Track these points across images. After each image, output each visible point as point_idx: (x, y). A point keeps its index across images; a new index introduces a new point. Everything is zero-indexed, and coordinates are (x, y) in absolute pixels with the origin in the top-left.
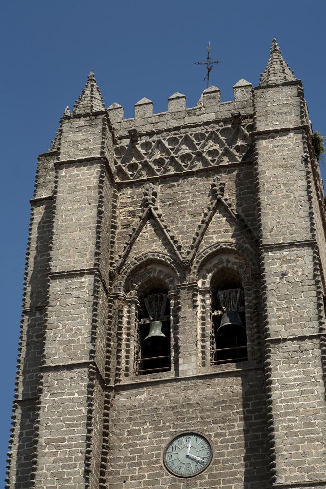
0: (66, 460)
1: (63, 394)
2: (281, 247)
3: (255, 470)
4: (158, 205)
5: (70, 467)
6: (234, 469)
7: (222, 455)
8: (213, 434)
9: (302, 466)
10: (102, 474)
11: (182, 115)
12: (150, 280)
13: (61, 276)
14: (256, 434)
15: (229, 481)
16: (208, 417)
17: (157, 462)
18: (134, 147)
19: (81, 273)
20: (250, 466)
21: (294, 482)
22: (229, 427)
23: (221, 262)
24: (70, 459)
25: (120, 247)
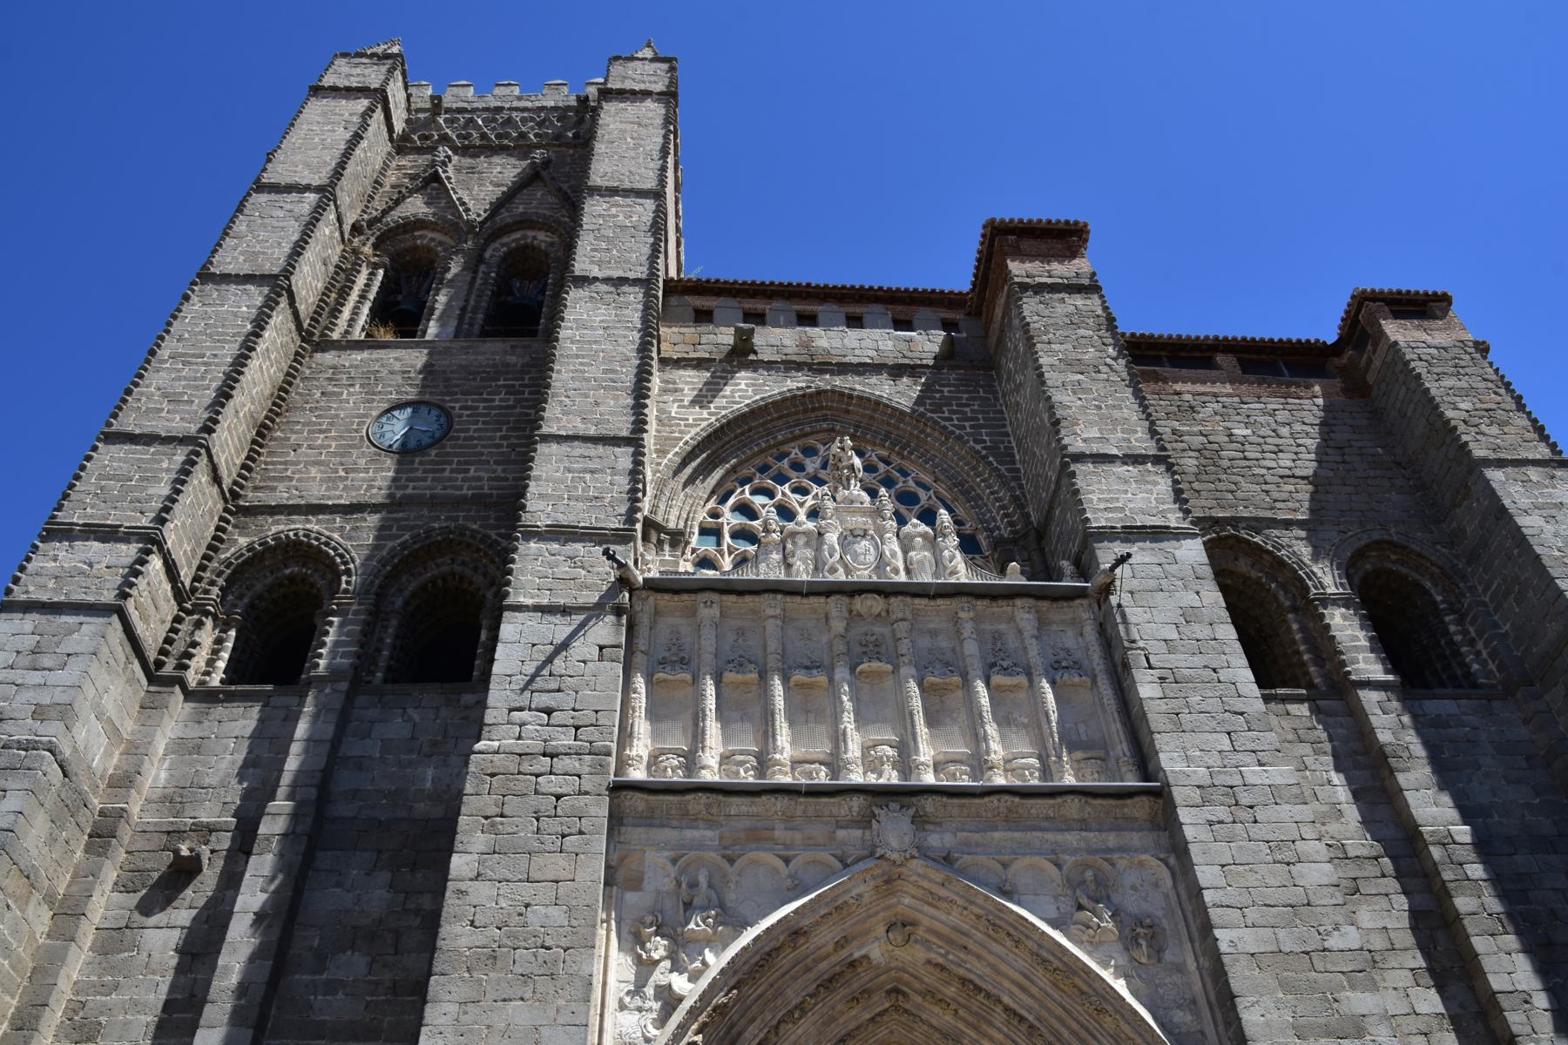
0: (195, 379)
1: (223, 305)
2: (613, 191)
4: (450, 168)
5: (197, 388)
6: (479, 449)
7: (467, 430)
8: (458, 405)
10: (259, 434)
11: (510, 99)
12: (416, 248)
13: (275, 188)
15: (467, 463)
16: (457, 386)
17: (356, 431)
18: (435, 121)
19: (307, 188)
22: (485, 400)
23: (525, 237)
24: (203, 378)
25: (379, 204)
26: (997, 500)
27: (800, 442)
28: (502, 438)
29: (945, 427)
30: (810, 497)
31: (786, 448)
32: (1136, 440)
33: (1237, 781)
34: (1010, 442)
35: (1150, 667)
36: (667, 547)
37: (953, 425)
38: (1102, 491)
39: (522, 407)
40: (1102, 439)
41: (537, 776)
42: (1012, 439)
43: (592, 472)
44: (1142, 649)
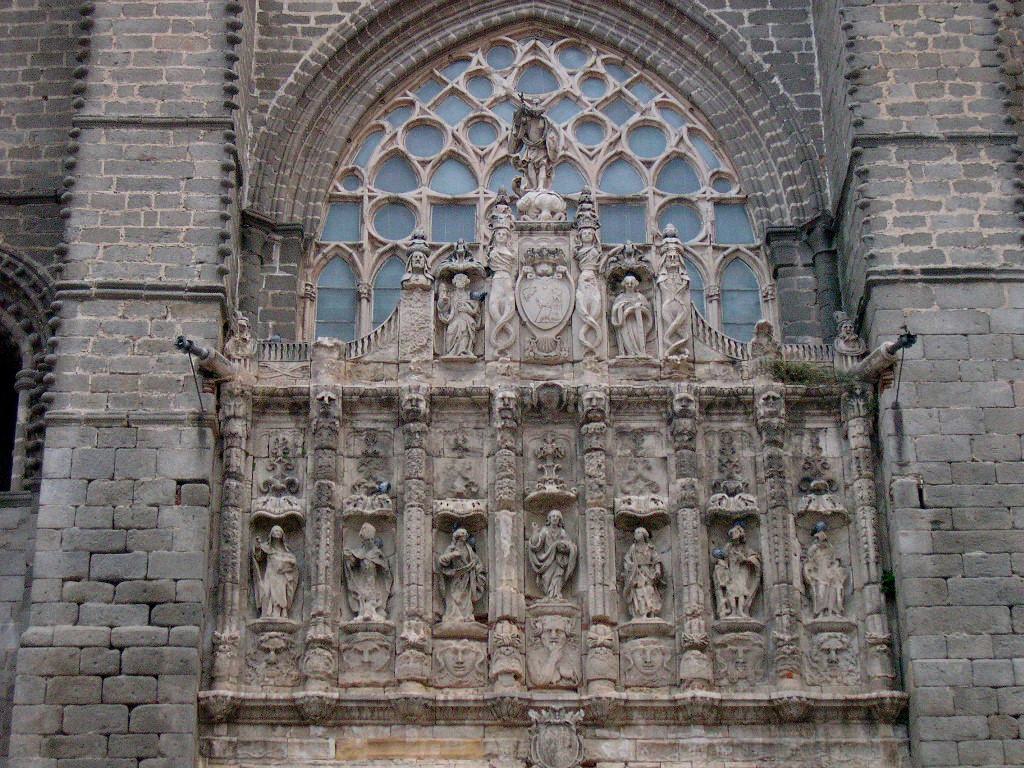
3: (45, 103)
9: (152, 83)
14: (62, 23)
20: (35, 93)
21: (125, 115)
26: (779, 152)
27: (484, 42)
28: (30, 75)
29: (710, 16)
30: (495, 144)
31: (465, 51)
32: (971, 107)
33: (1005, 678)
34: (809, 46)
35: (923, 506)
36: (276, 255)
37: (722, 15)
38: (902, 205)
39: (54, 15)
40: (919, 109)
41: (104, 676)
42: (813, 39)
43: (159, 186)
44: (917, 476)
